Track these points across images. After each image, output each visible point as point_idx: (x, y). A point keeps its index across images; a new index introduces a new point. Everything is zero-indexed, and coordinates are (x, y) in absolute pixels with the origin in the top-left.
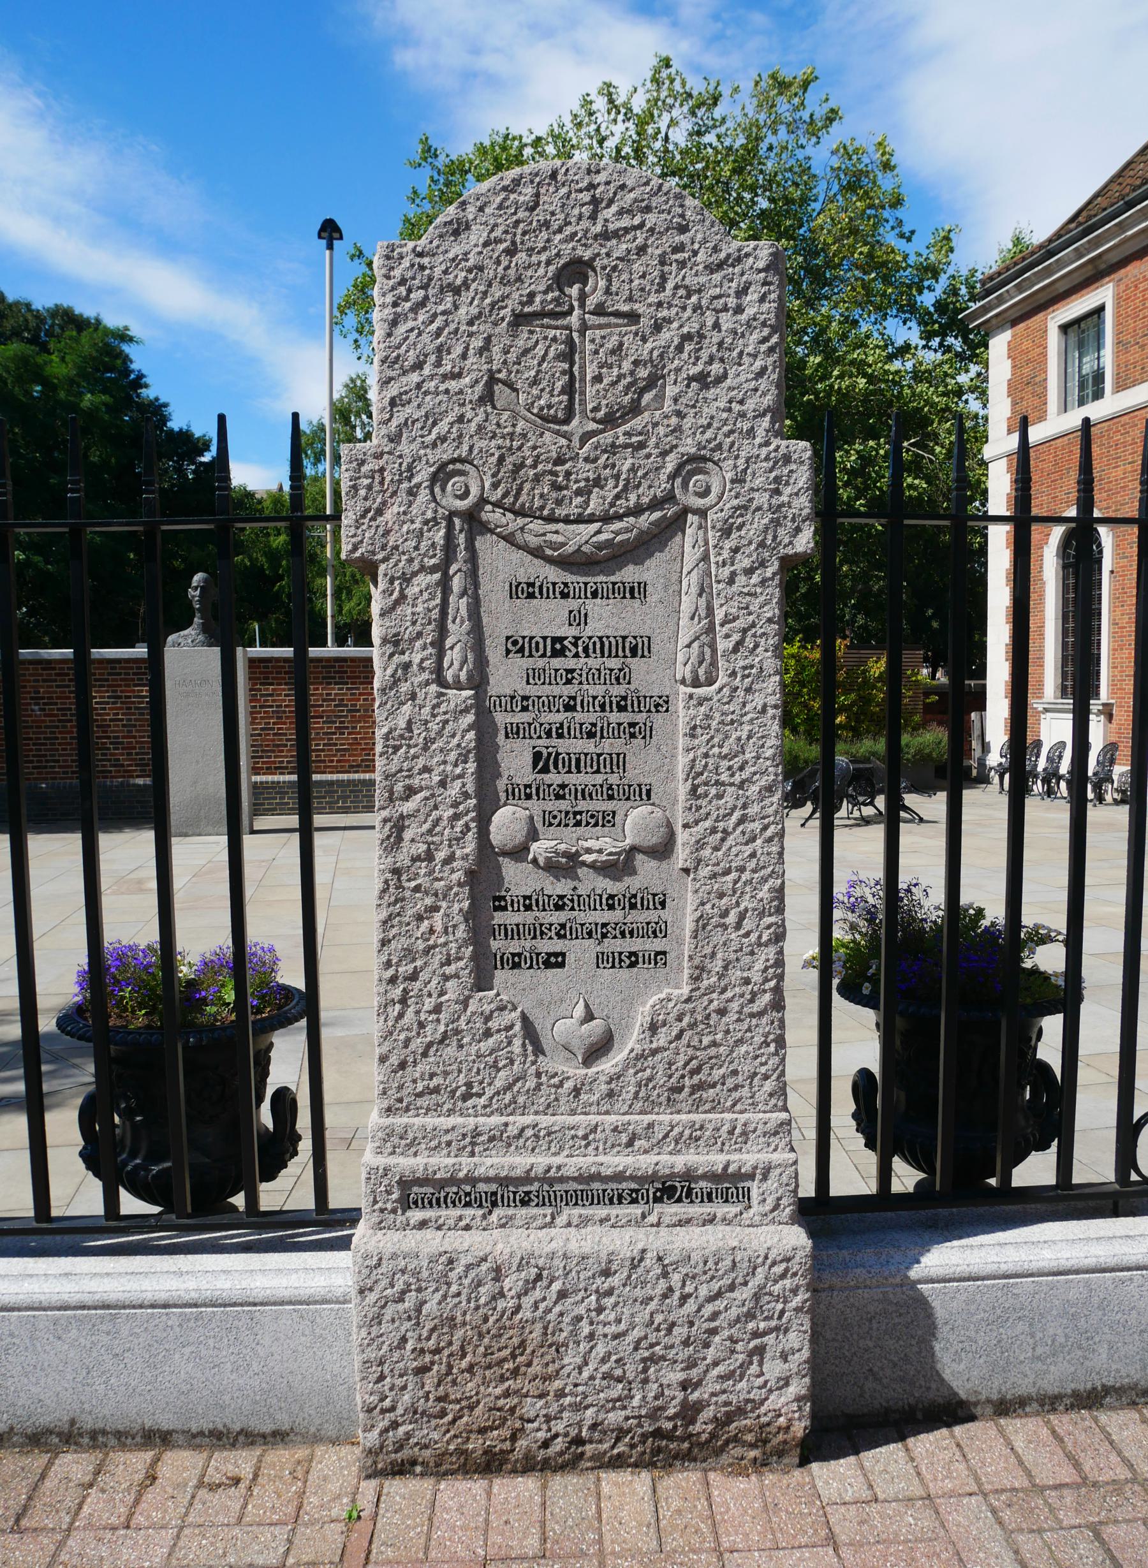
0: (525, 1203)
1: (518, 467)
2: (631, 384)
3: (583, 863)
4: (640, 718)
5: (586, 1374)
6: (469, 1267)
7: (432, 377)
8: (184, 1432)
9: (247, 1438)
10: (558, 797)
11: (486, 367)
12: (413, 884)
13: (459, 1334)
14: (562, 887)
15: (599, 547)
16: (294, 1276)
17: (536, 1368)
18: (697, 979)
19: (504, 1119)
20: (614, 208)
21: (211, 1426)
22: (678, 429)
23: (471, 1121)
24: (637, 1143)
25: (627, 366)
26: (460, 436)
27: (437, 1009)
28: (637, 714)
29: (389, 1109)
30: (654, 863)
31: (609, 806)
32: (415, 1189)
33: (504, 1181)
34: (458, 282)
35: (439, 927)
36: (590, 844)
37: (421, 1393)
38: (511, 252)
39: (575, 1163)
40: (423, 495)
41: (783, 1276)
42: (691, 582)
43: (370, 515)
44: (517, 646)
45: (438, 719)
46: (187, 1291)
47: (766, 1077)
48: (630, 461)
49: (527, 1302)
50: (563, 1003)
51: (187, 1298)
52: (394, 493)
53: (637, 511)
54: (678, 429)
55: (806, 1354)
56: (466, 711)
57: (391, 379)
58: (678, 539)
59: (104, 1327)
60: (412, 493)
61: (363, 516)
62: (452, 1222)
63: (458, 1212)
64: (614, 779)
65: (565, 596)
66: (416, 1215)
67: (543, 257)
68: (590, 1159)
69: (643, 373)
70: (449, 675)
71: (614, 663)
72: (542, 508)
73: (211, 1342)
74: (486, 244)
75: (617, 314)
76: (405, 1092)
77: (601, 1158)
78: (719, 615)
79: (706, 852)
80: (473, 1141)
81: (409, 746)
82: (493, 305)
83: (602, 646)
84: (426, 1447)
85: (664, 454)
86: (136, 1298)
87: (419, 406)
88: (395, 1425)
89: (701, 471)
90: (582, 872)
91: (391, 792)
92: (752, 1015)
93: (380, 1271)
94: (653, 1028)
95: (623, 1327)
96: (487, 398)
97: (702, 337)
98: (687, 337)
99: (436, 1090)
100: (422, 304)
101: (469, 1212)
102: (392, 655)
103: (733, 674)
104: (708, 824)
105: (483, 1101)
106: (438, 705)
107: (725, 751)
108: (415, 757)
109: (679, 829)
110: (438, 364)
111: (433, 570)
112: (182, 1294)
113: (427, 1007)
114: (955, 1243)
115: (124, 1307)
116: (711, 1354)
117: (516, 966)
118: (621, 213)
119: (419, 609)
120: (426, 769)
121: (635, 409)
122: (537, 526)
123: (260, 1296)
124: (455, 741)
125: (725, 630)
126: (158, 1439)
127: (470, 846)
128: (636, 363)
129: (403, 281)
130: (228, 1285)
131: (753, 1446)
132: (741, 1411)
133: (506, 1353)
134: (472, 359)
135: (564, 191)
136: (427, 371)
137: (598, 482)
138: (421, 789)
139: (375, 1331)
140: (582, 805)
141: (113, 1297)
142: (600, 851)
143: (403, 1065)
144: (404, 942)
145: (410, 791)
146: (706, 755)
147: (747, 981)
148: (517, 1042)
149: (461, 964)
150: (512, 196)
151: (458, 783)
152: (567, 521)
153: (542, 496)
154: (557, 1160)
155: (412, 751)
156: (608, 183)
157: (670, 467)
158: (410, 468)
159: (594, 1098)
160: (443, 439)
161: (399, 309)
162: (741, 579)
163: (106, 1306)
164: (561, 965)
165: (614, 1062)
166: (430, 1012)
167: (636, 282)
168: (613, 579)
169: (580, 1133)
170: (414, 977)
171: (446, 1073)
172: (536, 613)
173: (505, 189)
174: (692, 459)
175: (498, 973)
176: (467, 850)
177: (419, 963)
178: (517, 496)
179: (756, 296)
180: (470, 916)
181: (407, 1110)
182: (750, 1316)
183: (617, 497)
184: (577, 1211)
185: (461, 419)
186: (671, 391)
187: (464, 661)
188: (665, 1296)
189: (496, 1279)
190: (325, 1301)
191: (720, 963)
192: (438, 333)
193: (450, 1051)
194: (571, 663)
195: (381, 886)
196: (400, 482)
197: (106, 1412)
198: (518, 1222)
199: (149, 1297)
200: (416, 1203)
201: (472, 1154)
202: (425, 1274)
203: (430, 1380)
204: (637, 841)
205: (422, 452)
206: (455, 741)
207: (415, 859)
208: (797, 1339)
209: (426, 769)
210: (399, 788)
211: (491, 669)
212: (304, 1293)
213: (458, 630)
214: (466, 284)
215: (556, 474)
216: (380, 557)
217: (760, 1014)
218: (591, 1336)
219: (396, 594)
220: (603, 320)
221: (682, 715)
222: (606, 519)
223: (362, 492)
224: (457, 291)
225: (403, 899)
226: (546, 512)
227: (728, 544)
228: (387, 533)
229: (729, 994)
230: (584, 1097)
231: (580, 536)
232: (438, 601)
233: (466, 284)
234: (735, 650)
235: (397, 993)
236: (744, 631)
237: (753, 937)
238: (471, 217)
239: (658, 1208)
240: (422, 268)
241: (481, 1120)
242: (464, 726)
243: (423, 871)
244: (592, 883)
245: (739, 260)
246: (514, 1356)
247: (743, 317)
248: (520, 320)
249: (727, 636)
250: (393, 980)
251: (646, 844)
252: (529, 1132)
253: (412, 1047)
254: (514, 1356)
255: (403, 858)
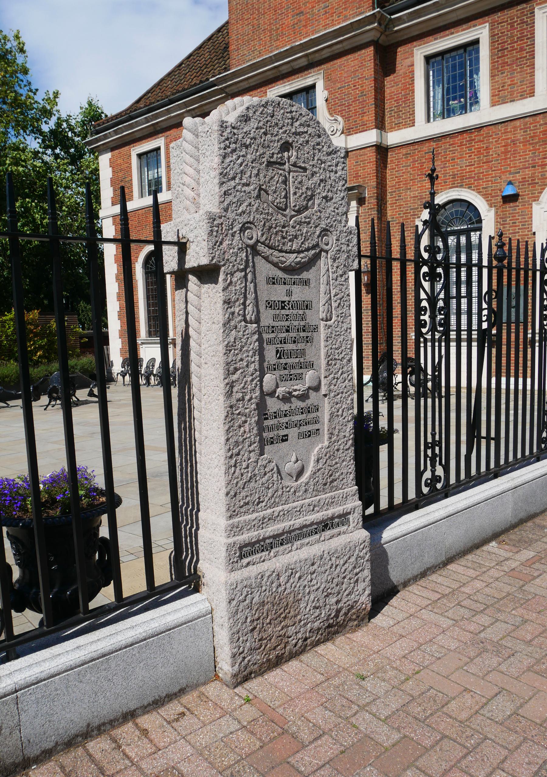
0: (282, 544)
1: (271, 227)
2: (306, 197)
3: (294, 396)
4: (309, 334)
5: (308, 609)
6: (269, 577)
7: (239, 184)
8: (141, 707)
9: (170, 697)
10: (285, 369)
11: (258, 183)
12: (237, 412)
13: (266, 607)
14: (286, 407)
15: (297, 263)
16: (182, 611)
17: (292, 613)
18: (330, 438)
19: (272, 510)
20: (298, 123)
21: (153, 699)
22: (320, 217)
23: (261, 514)
24: (315, 509)
25: (304, 189)
26: (250, 212)
27: (247, 467)
28: (308, 332)
29: (230, 517)
30: (315, 393)
31: (300, 371)
32: (244, 549)
33: (274, 537)
34: (248, 143)
35: (247, 430)
36: (295, 387)
37: (253, 640)
38: (265, 134)
39: (298, 522)
40: (237, 235)
41: (363, 549)
42: (323, 280)
43: (218, 244)
44: (270, 305)
45: (245, 337)
46: (140, 633)
47: (351, 473)
48: (306, 229)
49: (288, 585)
50: (286, 455)
51: (141, 637)
52: (227, 235)
53: (308, 250)
54: (320, 217)
55: (370, 577)
56: (255, 333)
57: (224, 183)
58: (319, 262)
59: (103, 667)
60: (233, 236)
61: (215, 245)
62: (258, 560)
63: (260, 555)
64: (302, 360)
65: (285, 284)
66: (245, 561)
67: (277, 138)
68: (302, 519)
69: (309, 193)
70: (248, 318)
71: (301, 312)
72: (278, 246)
73: (152, 656)
74: (257, 128)
75: (300, 167)
76: (236, 506)
77: (305, 518)
78: (333, 293)
79: (332, 387)
80: (263, 522)
81: (235, 350)
82: (260, 155)
83: (296, 305)
84: (256, 664)
85: (316, 227)
86: (117, 646)
87: (235, 196)
88: (244, 658)
89: (250, 228)
90: (293, 399)
91: (229, 371)
92: (347, 450)
93: (237, 589)
94: (318, 461)
95: (319, 585)
96: (258, 197)
97: (326, 181)
98: (321, 181)
99: (247, 504)
100: (234, 151)
101: (264, 553)
102: (227, 309)
103: (338, 316)
104: (332, 376)
105: (264, 504)
106: (244, 331)
107: (337, 346)
108: (237, 354)
109: (322, 379)
110: (241, 179)
111: (242, 270)
112: (138, 636)
113: (244, 466)
114: (393, 525)
115: (112, 653)
116: (344, 586)
117: (272, 443)
118: (301, 125)
119: (237, 288)
120: (242, 360)
121: (306, 208)
122: (276, 253)
123: (172, 624)
124: (251, 347)
125: (335, 299)
126: (130, 716)
127: (258, 393)
128: (307, 188)
129: (227, 139)
130: (157, 625)
131: (355, 620)
132: (352, 607)
133: (283, 609)
134: (253, 179)
135: (282, 111)
136: (237, 181)
137: (296, 237)
138: (240, 368)
139: (235, 618)
140: (293, 372)
141: (107, 649)
142: (299, 390)
143: (235, 496)
144: (235, 438)
145: (236, 370)
146: (331, 348)
147: (345, 436)
148: (275, 475)
149: (255, 445)
150: (266, 109)
151: (253, 365)
152: (286, 252)
153: (278, 241)
154: (292, 523)
155: (236, 352)
156: (296, 112)
157: (318, 233)
158: (232, 224)
159: (301, 494)
160: (244, 212)
161: (226, 151)
162: (339, 278)
163: (104, 656)
164: (287, 440)
165: (305, 477)
166: (245, 469)
167: (306, 155)
168: (300, 277)
169: (298, 509)
170: (238, 454)
171: (251, 494)
172: (276, 291)
173: (263, 105)
174: (325, 230)
175: (266, 447)
176: (257, 394)
177: (240, 447)
178: (270, 240)
179: (341, 168)
180: (258, 423)
181: (237, 514)
182: (355, 567)
183: (302, 243)
184: (299, 542)
185: (250, 204)
186: (317, 202)
187: (253, 312)
188: (331, 568)
189: (278, 579)
190: (199, 617)
191: (337, 431)
192: (241, 165)
193: (252, 484)
194: (287, 312)
195: (226, 414)
196: (229, 230)
197: (105, 712)
198: (280, 553)
199: (124, 643)
200: (244, 556)
201: (263, 528)
202: (254, 585)
203: (256, 633)
204: (311, 385)
205: (236, 217)
206: (251, 347)
207: (238, 400)
208: (367, 573)
209: (242, 360)
210: (232, 368)
211: (261, 315)
212: (190, 617)
213: (251, 297)
214: (250, 145)
215: (282, 232)
216: (222, 263)
217: (349, 449)
218: (309, 593)
219: (228, 281)
220: (295, 169)
221: (323, 333)
222: (299, 252)
223: (215, 233)
224: (247, 147)
225: (233, 419)
226: (280, 248)
227: (335, 265)
228: (224, 252)
229: (340, 443)
230: (297, 494)
231: (291, 259)
232: (244, 285)
233: (250, 145)
234: (338, 307)
235: (233, 462)
236: (341, 299)
237: (346, 418)
238: (251, 115)
239: (323, 534)
240: (235, 134)
241: (265, 512)
242: (255, 340)
243: (241, 405)
244: (297, 404)
245: (336, 152)
246: (284, 611)
247: (337, 175)
248: (270, 164)
249: (336, 301)
250: (231, 457)
251: (314, 385)
252: (281, 513)
253: (239, 485)
254: (284, 611)
255: (233, 401)
